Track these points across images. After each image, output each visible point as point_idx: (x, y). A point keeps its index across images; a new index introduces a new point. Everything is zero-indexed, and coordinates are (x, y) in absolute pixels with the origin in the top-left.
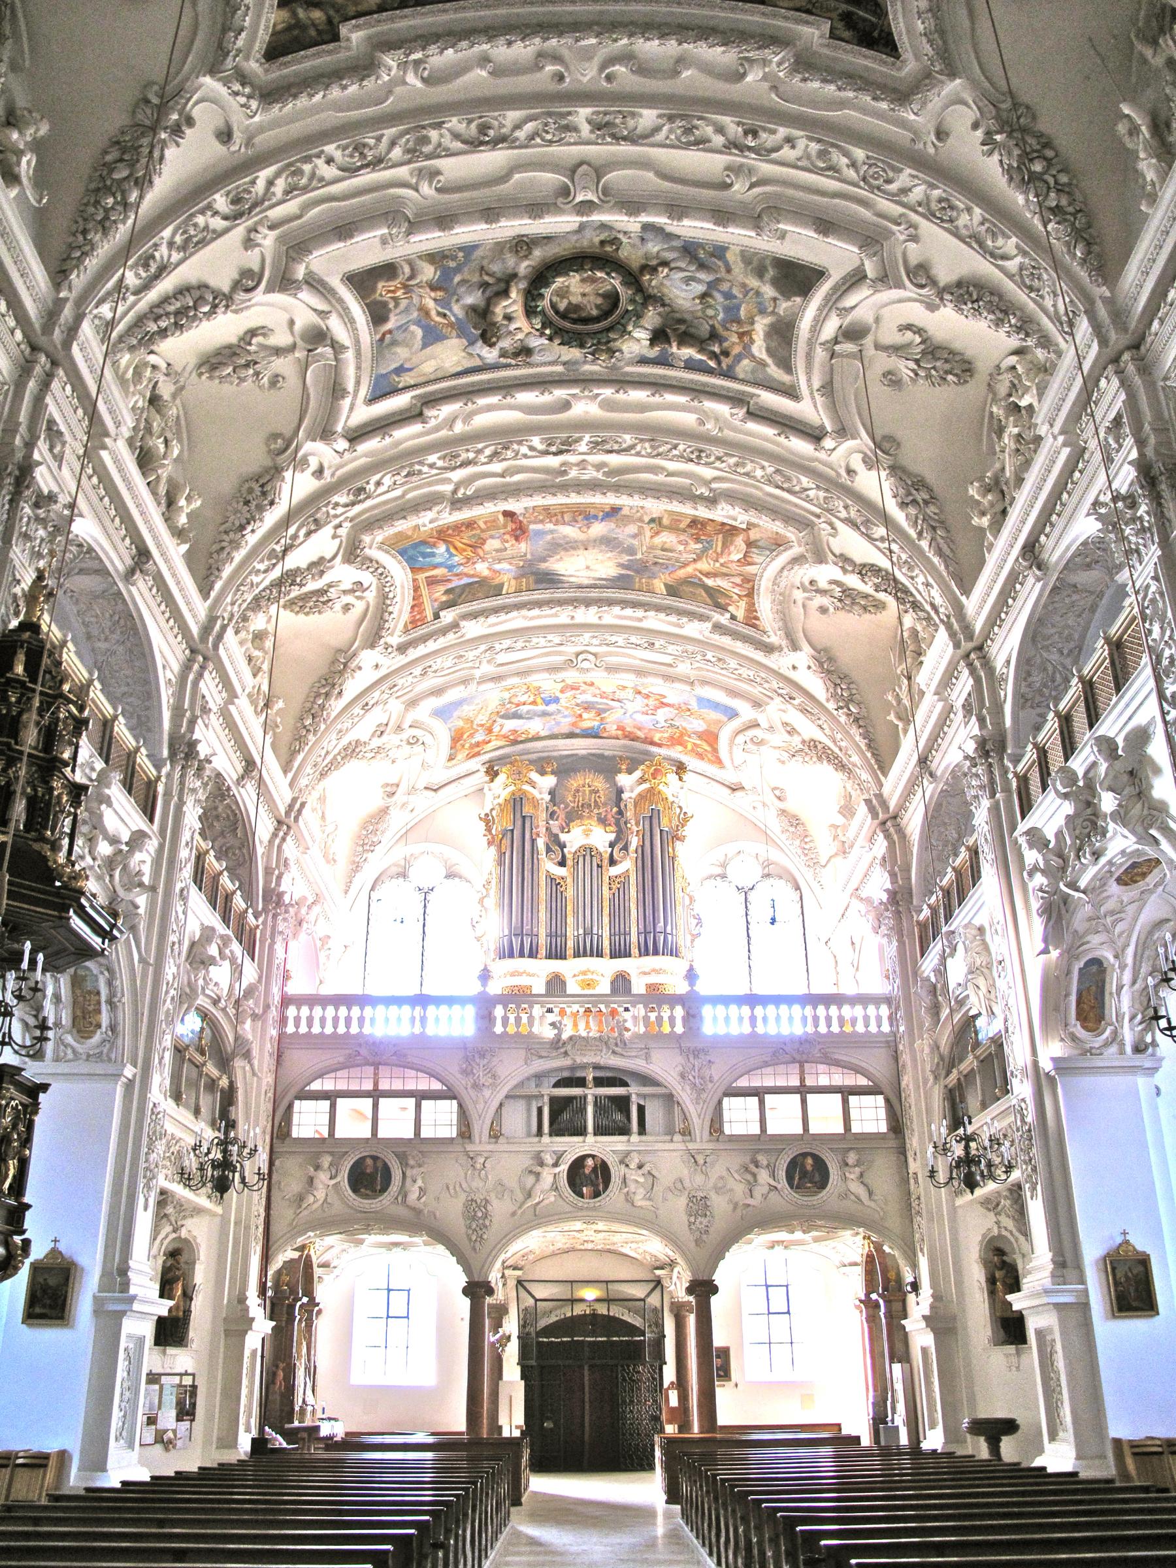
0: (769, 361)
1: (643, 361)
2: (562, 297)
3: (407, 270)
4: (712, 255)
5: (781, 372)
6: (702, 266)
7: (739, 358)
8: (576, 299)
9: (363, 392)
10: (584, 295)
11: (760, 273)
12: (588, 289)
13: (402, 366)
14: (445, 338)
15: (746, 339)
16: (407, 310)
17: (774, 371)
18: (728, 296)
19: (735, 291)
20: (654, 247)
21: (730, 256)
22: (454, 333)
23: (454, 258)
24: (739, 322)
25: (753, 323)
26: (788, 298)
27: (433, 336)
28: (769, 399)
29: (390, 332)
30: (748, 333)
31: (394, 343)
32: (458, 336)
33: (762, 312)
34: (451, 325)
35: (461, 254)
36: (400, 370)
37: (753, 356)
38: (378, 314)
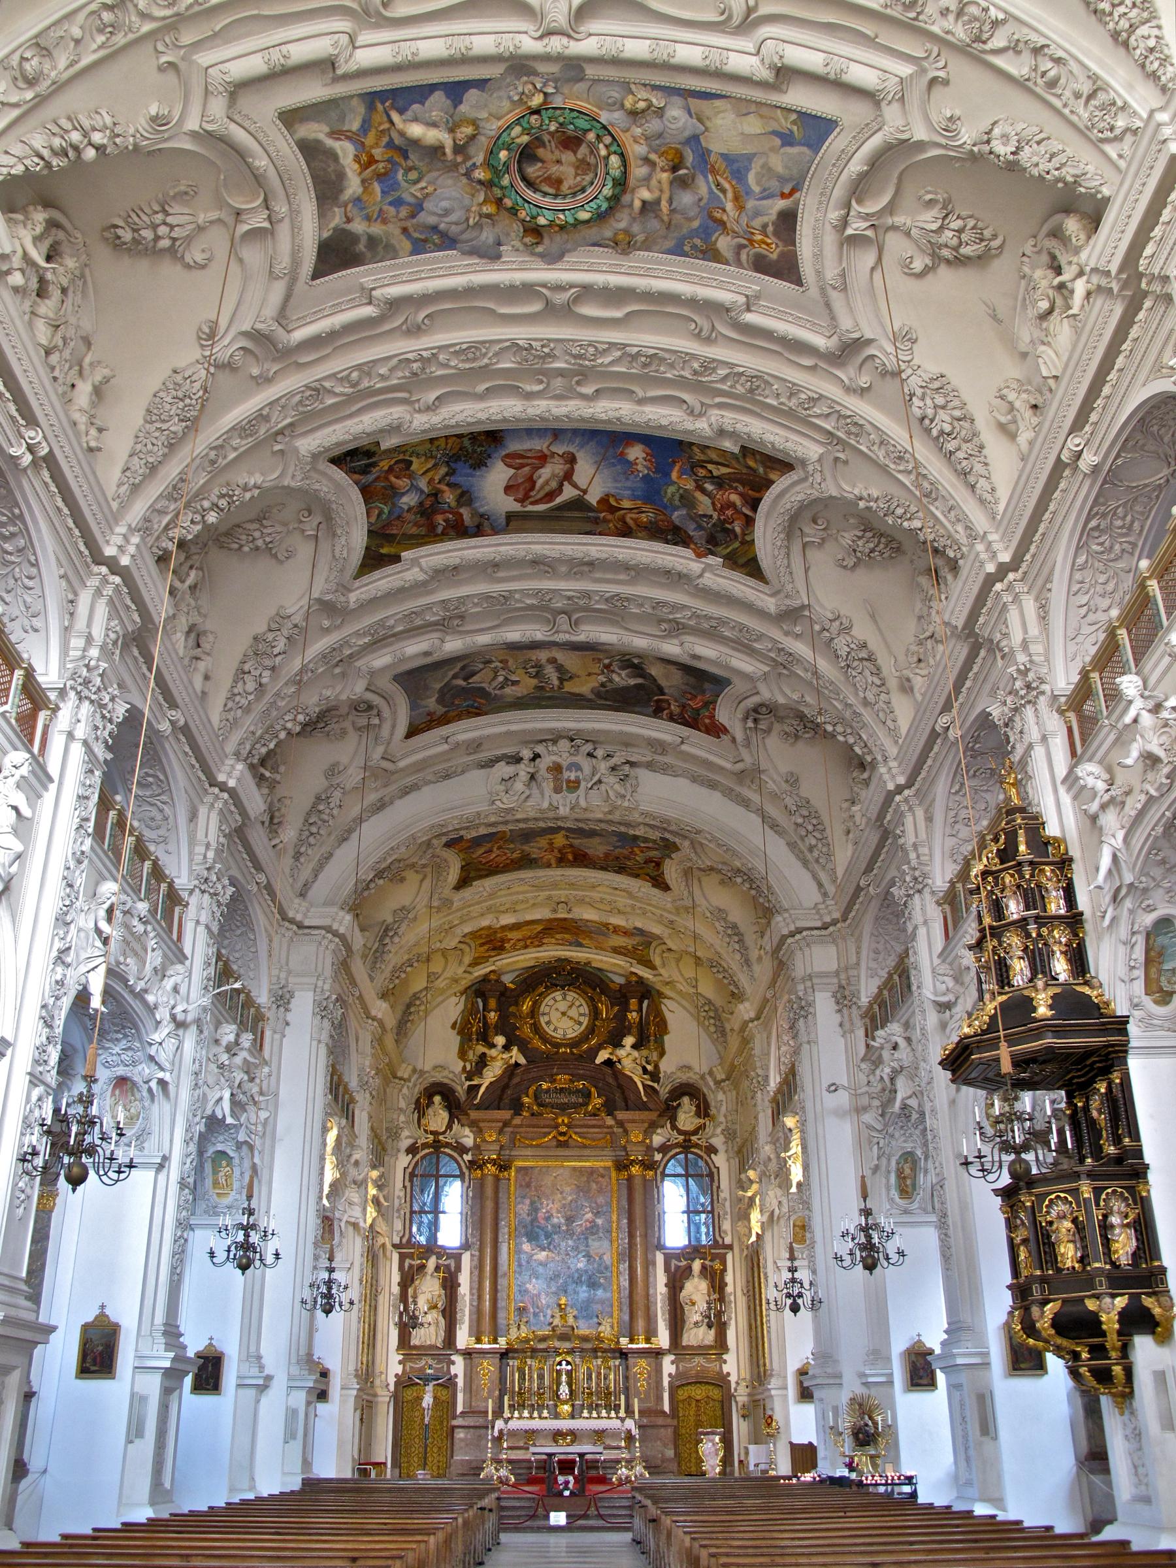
0: (330, 142)
1: (481, 84)
2: (583, 161)
3: (744, 257)
4: (425, 241)
5: (312, 136)
6: (434, 228)
7: (365, 127)
8: (568, 157)
9: (836, 143)
10: (558, 162)
11: (372, 241)
12: (554, 169)
13: (783, 145)
14: (724, 156)
15: (364, 158)
16: (757, 213)
17: (316, 131)
18: (398, 203)
19: (392, 210)
20: (487, 236)
21: (407, 245)
22: (713, 159)
23: (694, 247)
24: (380, 177)
25: (363, 181)
26: (335, 229)
27: (737, 166)
28: (314, 91)
29: (783, 196)
30: (364, 167)
31: (782, 180)
32: (709, 152)
33: (357, 200)
34: (714, 171)
35: (687, 248)
36: (787, 139)
37: (349, 138)
38: (788, 221)
